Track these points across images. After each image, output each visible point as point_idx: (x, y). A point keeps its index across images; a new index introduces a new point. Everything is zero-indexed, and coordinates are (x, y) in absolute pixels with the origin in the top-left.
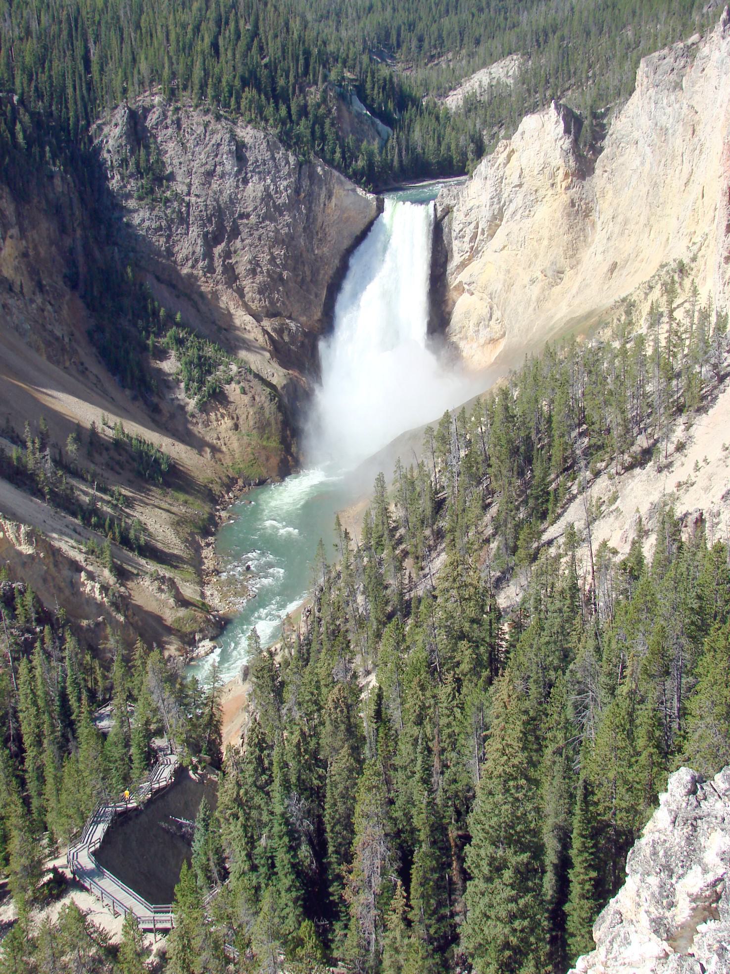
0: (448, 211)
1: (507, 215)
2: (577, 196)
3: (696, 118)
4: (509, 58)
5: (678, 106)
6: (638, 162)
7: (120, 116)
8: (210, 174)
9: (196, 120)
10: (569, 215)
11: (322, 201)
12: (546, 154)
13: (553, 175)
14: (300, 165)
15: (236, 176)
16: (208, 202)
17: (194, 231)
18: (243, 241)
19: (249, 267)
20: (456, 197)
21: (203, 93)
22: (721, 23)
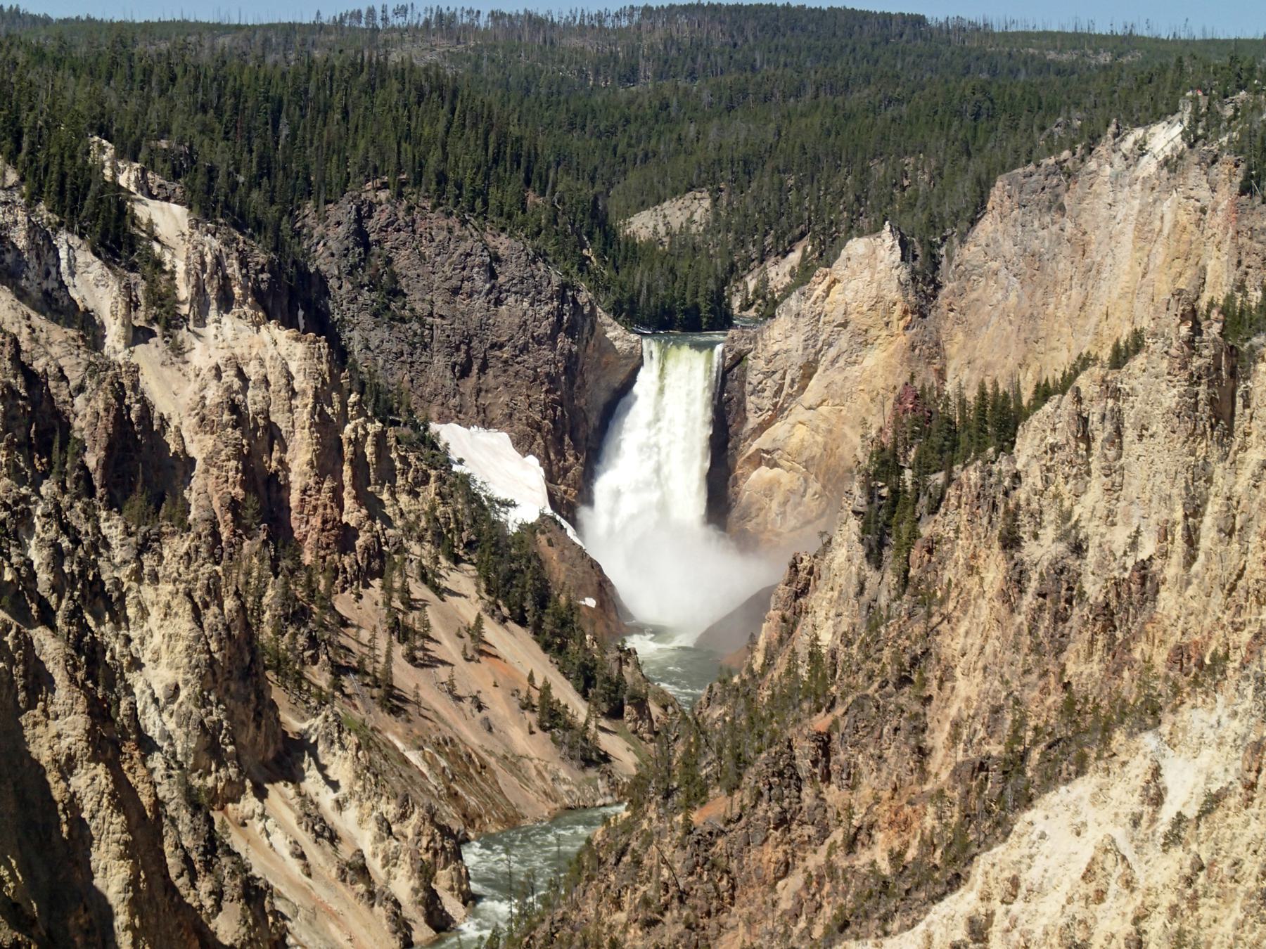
0: (740, 359)
1: (824, 362)
2: (918, 338)
3: (1086, 238)
4: (689, 195)
5: (1057, 226)
6: (999, 296)
7: (343, 211)
8: (456, 291)
9: (436, 223)
10: (910, 360)
11: (585, 336)
12: (880, 285)
13: (889, 312)
14: (564, 286)
15: (487, 294)
16: (456, 325)
17: (439, 361)
18: (496, 377)
19: (506, 411)
20: (753, 339)
21: (441, 193)
22: (1109, 136)
